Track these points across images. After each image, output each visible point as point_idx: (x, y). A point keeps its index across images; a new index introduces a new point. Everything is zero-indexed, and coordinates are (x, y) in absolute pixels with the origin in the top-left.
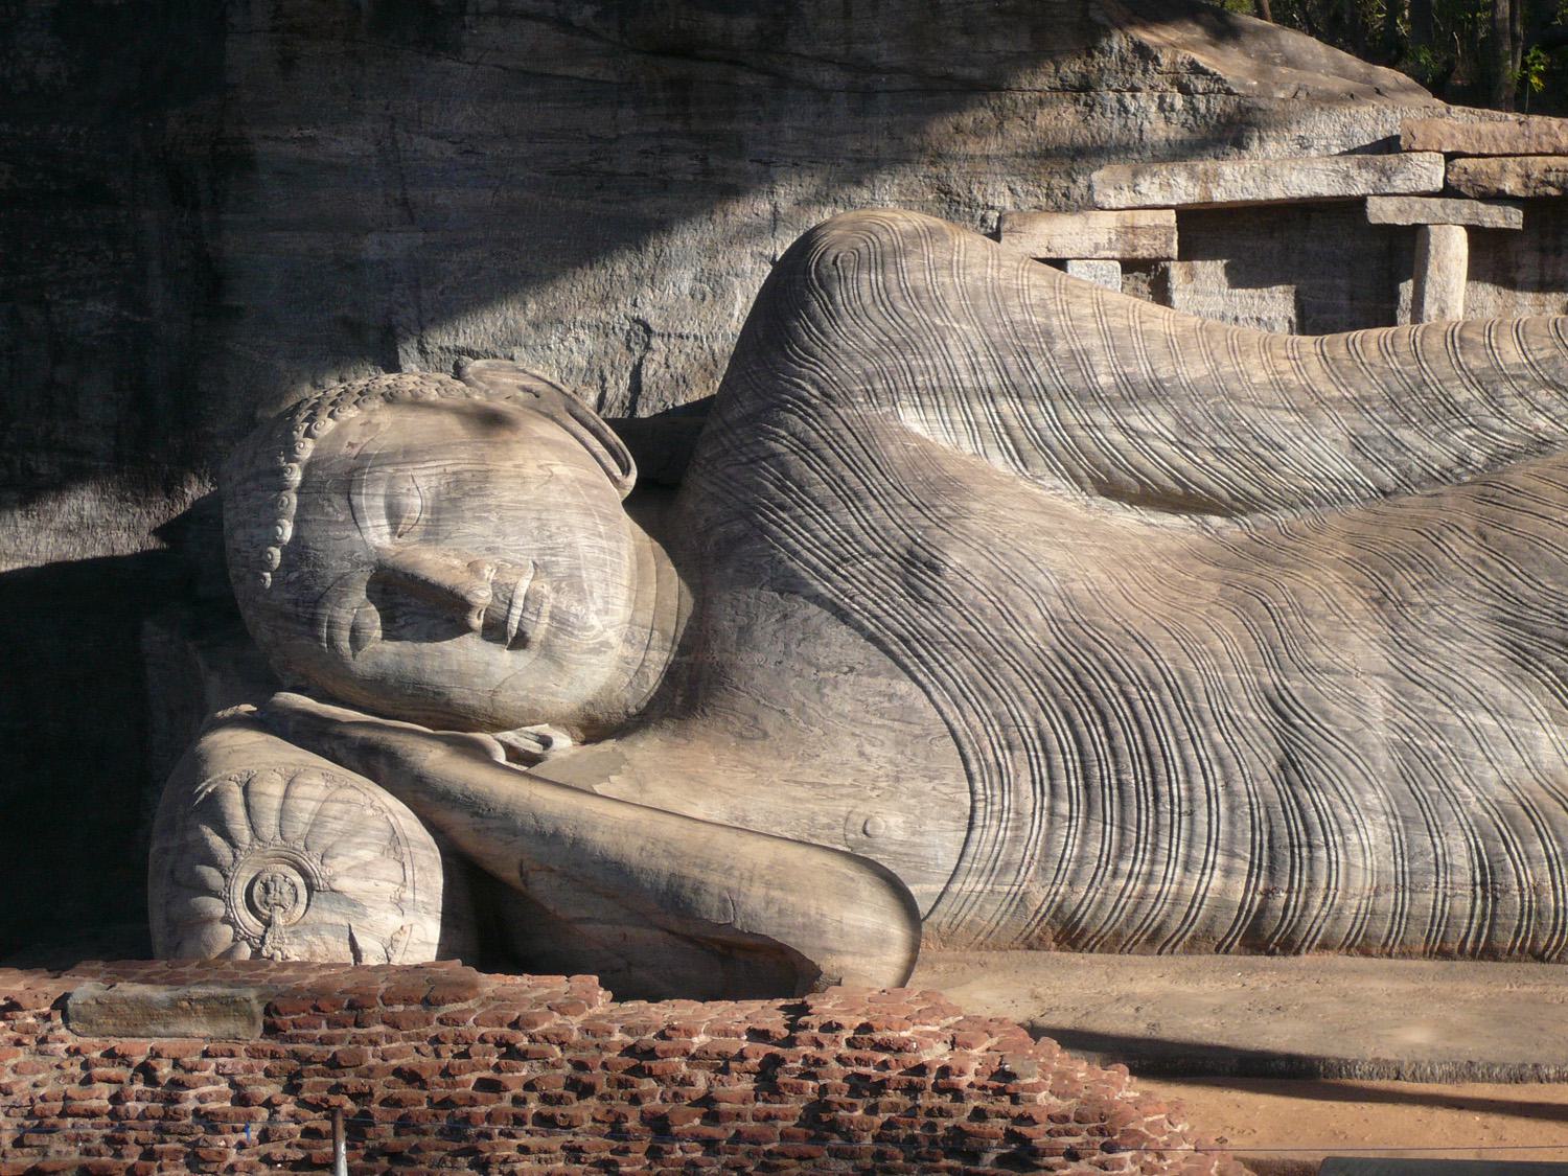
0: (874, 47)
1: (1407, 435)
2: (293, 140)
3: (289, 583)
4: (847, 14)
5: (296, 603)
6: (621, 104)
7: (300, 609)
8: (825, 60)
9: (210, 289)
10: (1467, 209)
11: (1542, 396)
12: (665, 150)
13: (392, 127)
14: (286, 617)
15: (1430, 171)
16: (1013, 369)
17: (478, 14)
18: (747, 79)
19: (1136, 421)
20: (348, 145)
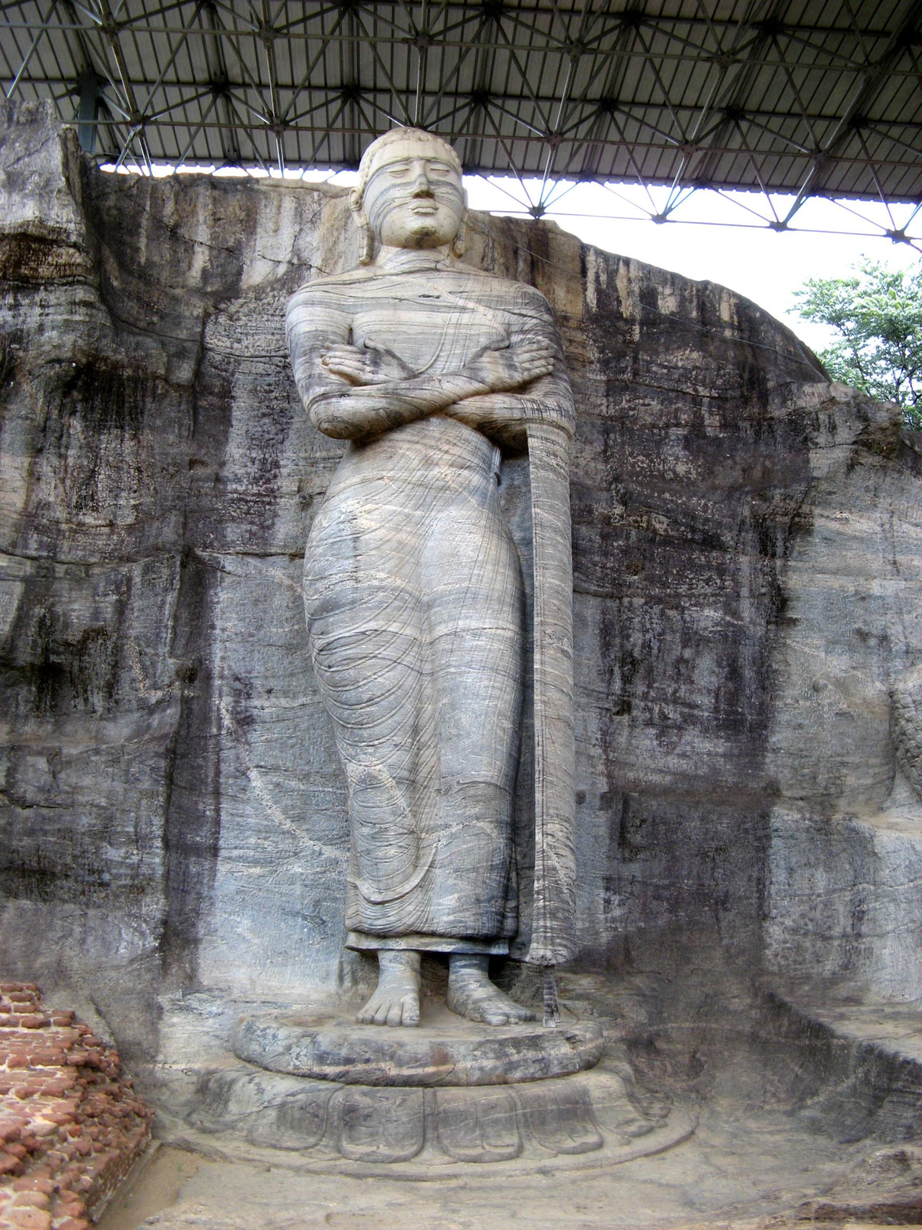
2: (836, 519)
9: (779, 607)
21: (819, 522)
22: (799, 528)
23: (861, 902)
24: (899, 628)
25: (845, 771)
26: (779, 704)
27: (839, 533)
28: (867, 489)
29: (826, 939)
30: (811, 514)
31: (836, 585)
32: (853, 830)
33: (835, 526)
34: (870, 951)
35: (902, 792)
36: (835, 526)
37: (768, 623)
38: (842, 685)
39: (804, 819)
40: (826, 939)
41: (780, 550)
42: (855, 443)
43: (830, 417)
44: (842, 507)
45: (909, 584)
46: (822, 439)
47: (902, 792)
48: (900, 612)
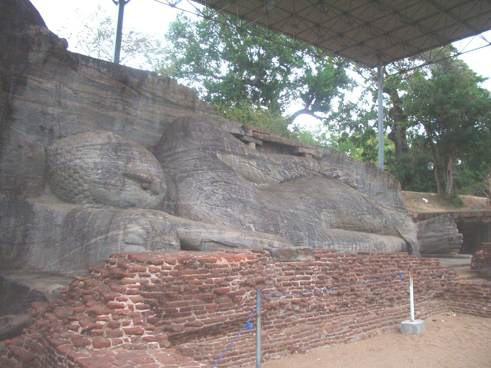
0: (157, 92)
1: (286, 171)
2: (37, 81)
3: (98, 173)
4: (153, 84)
5: (100, 179)
6: (109, 91)
7: (101, 181)
8: (147, 91)
10: (256, 141)
11: (302, 168)
12: (117, 102)
13: (60, 84)
14: (96, 182)
15: (251, 133)
16: (233, 148)
17: (81, 64)
18: (133, 91)
19: (251, 162)
20: (49, 85)
21: (30, 81)
22: (21, 82)
23: (27, 230)
24: (58, 127)
25: (28, 180)
26: (4, 151)
27: (38, 87)
28: (51, 71)
29: (13, 245)
30: (27, 78)
31: (34, 107)
32: (26, 202)
33: (36, 84)
34: (28, 249)
35: (47, 189)
36: (36, 84)
37: (3, 118)
38: (32, 147)
39: (7, 197)
40: (13, 245)
41: (11, 90)
42: (47, 52)
43: (39, 39)
44: (40, 77)
45: (64, 111)
46: (34, 48)
47: (47, 189)
48: (59, 121)
